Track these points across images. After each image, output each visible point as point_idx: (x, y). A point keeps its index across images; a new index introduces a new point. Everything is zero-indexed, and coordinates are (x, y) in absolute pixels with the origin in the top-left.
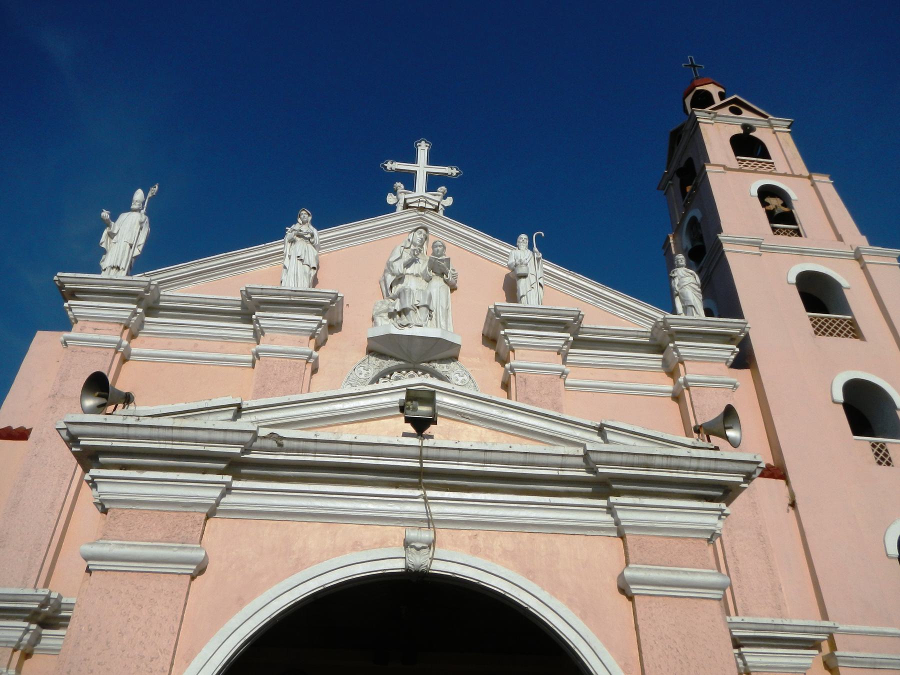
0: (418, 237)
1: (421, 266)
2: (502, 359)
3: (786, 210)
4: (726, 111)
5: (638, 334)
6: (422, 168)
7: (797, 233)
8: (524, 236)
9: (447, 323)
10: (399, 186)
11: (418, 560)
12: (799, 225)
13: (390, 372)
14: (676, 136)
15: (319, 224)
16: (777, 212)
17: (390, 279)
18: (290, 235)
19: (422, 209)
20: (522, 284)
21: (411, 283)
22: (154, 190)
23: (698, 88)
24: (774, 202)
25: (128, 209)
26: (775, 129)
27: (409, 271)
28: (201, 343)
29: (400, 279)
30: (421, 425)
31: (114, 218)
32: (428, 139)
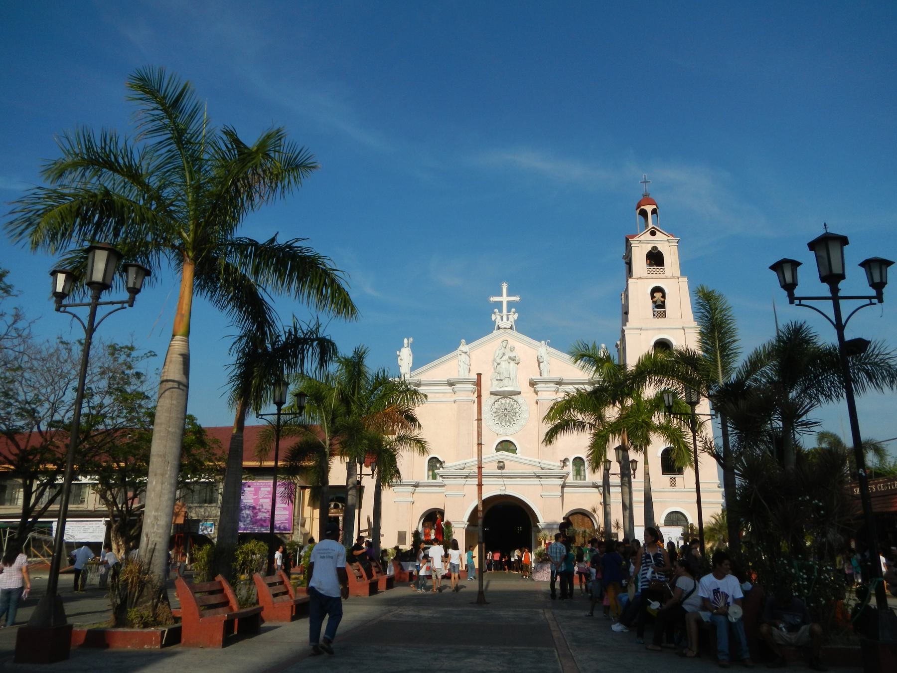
0: (505, 344)
1: (506, 357)
2: (536, 392)
3: (662, 299)
4: (647, 236)
5: (584, 380)
6: (505, 299)
7: (663, 315)
8: (543, 342)
9: (516, 381)
10: (496, 310)
11: (503, 493)
12: (666, 309)
13: (499, 400)
15: (467, 344)
16: (657, 304)
17: (496, 364)
18: (457, 352)
19: (505, 328)
20: (542, 364)
21: (504, 365)
23: (642, 207)
24: (658, 295)
25: (403, 346)
27: (502, 359)
28: (437, 395)
29: (499, 364)
30: (501, 468)
31: (400, 352)
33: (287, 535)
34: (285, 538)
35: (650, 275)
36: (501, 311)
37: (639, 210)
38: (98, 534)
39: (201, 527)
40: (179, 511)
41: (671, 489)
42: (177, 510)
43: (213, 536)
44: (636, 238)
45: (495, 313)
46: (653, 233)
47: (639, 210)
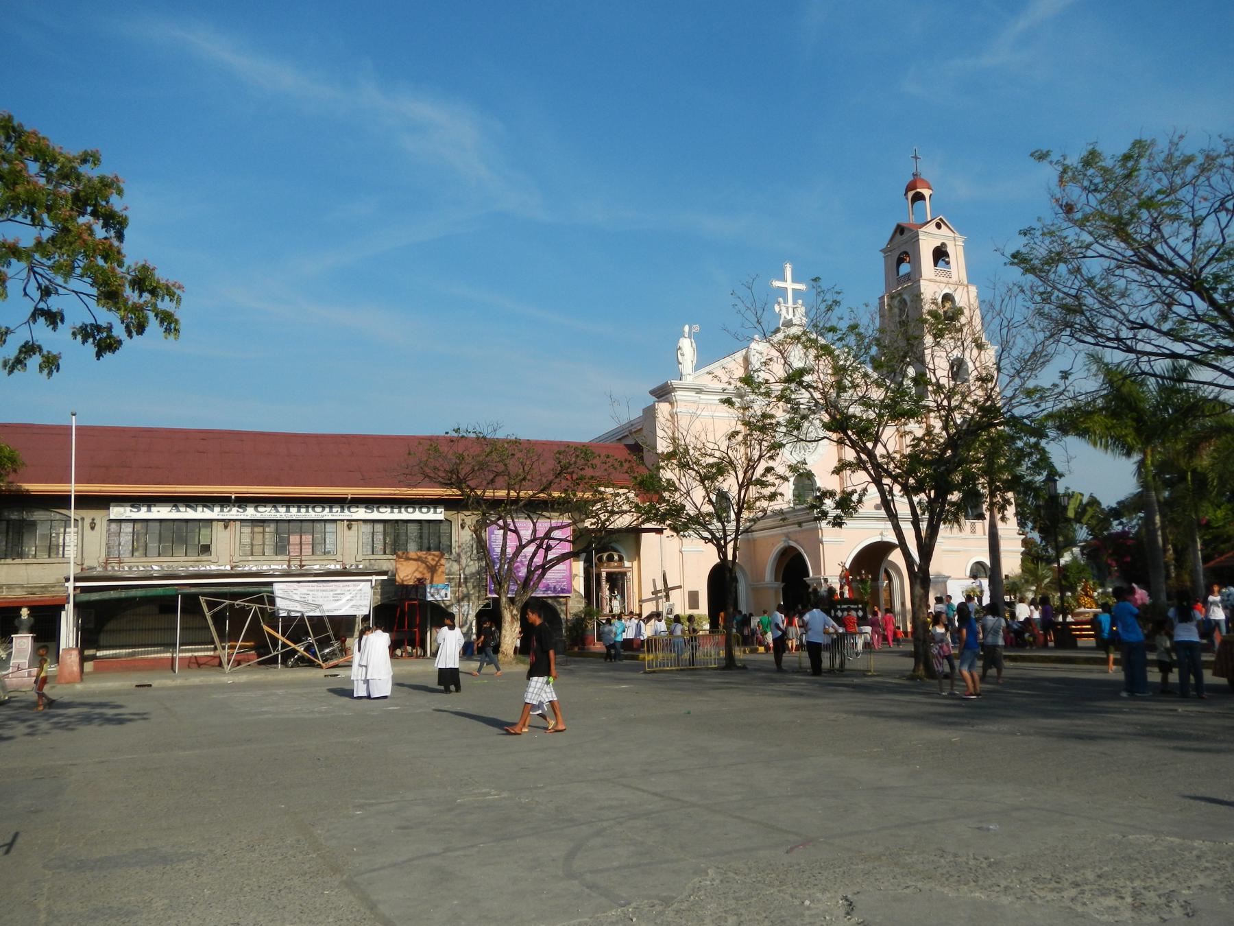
6: (790, 285)
10: (781, 300)
14: (900, 230)
22: (697, 328)
23: (919, 190)
26: (957, 243)
32: (792, 262)
33: (561, 600)
34: (560, 603)
35: (938, 278)
36: (786, 302)
37: (913, 192)
38: (360, 603)
39: (428, 590)
40: (436, 565)
41: (972, 536)
42: (434, 563)
43: (448, 603)
44: (923, 229)
45: (779, 303)
46: (938, 226)
47: (913, 192)
